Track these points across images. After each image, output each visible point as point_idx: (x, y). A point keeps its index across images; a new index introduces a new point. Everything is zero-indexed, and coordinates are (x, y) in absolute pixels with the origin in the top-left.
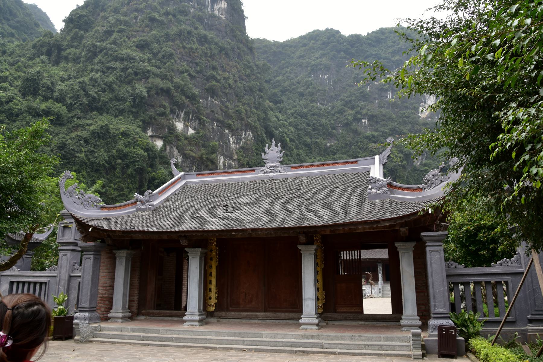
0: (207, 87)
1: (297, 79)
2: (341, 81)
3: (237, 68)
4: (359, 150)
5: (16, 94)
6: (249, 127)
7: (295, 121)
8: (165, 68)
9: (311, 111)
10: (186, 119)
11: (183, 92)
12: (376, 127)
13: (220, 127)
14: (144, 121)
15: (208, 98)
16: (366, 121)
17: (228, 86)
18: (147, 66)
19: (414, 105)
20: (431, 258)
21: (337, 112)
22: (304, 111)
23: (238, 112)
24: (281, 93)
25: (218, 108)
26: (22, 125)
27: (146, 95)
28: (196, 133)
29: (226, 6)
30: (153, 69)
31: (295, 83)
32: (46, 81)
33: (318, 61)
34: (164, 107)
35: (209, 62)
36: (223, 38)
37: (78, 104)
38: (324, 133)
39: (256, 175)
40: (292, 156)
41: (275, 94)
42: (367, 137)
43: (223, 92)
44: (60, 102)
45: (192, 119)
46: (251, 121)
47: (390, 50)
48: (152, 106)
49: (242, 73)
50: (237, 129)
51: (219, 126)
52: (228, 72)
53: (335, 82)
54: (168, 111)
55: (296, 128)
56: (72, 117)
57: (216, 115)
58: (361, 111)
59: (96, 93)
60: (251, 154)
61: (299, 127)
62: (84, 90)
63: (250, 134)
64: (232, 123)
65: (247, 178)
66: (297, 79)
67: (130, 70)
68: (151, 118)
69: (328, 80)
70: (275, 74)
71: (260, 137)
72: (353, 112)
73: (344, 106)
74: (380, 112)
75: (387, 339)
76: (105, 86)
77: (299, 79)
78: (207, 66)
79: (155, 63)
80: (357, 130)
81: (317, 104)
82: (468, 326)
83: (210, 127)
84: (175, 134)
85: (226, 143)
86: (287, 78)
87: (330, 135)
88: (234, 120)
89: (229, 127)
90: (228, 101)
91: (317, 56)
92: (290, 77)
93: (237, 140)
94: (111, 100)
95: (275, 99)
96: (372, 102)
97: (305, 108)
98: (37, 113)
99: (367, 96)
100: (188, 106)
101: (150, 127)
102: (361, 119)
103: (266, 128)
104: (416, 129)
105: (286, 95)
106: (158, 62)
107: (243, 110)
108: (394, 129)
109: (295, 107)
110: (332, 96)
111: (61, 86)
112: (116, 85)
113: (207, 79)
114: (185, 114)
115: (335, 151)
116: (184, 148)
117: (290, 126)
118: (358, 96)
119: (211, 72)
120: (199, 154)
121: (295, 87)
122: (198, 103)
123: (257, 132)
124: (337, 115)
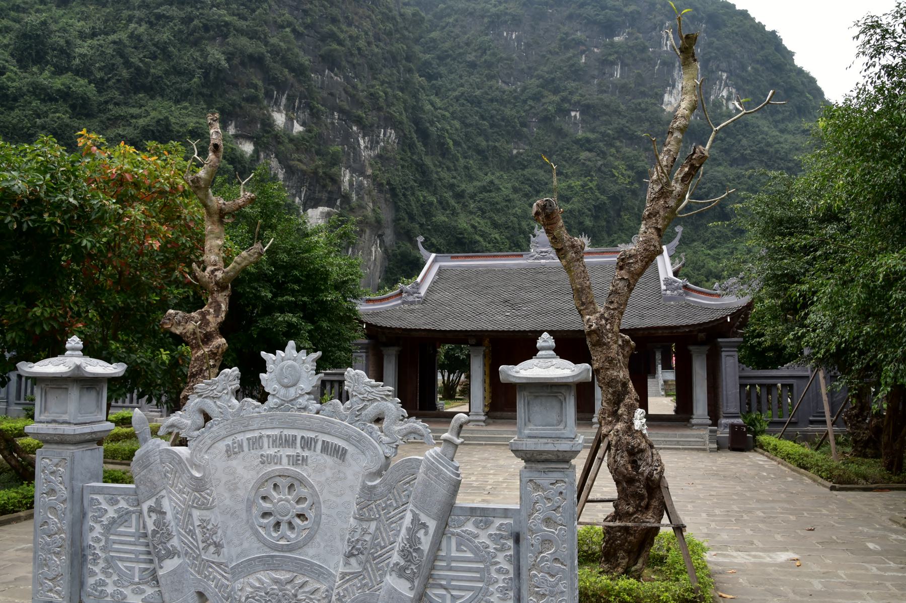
0: (322, 52)
1: (466, 37)
2: (538, 44)
3: (372, 20)
4: (564, 163)
5: (7, 61)
6: (390, 122)
7: (460, 111)
8: (254, 19)
9: (488, 94)
10: (290, 108)
11: (286, 63)
12: (593, 125)
13: (344, 121)
14: (222, 111)
15: (325, 71)
16: (578, 114)
17: (357, 52)
18: (225, 15)
19: (656, 90)
20: (725, 363)
21: (530, 98)
22: (476, 94)
23: (373, 96)
24: (438, 61)
25: (341, 89)
26: (26, 116)
27: (227, 65)
28: (306, 131)
30: (233, 19)
32: (57, 39)
34: (256, 87)
35: (326, 9)
37: (114, 81)
38: (508, 133)
39: (525, 262)
40: (456, 170)
41: (427, 64)
42: (577, 142)
43: (348, 62)
44: (83, 76)
45: (299, 108)
46: (394, 111)
48: (235, 85)
49: (380, 29)
50: (372, 126)
51: (342, 120)
52: (356, 26)
53: (528, 45)
54: (261, 95)
55: (463, 123)
56: (106, 102)
57: (338, 101)
58: (569, 97)
59: (141, 61)
60: (393, 167)
61: (468, 121)
62: (122, 56)
63: (392, 134)
65: (515, 265)
66: (466, 37)
67: (196, 22)
68: (233, 105)
71: (407, 139)
72: (556, 98)
73: (543, 87)
74: (601, 99)
75: (682, 436)
76: (155, 49)
77: (468, 38)
78: (321, 16)
79: (238, 10)
80: (562, 129)
81: (498, 82)
82: (755, 424)
83: (329, 121)
84: (273, 133)
85: (354, 149)
86: (448, 35)
87: (517, 136)
88: (367, 110)
89: (359, 121)
90: (356, 77)
92: (453, 34)
93: (371, 141)
94: (167, 73)
95: (427, 70)
96: (588, 82)
97: (478, 89)
98: (48, 95)
99: (580, 72)
100: (292, 86)
101: (231, 121)
102: (569, 111)
103: (417, 122)
104: (656, 130)
105: (446, 65)
106: (242, 7)
107: (381, 93)
108: (622, 130)
109: (462, 86)
110: (523, 69)
111: (83, 48)
112: (174, 47)
113: (324, 38)
114: (288, 99)
115: (526, 163)
116: (289, 156)
117: (454, 118)
118: (566, 72)
119: (328, 27)
120: (313, 166)
122: (309, 80)
123: (403, 131)
124: (530, 102)
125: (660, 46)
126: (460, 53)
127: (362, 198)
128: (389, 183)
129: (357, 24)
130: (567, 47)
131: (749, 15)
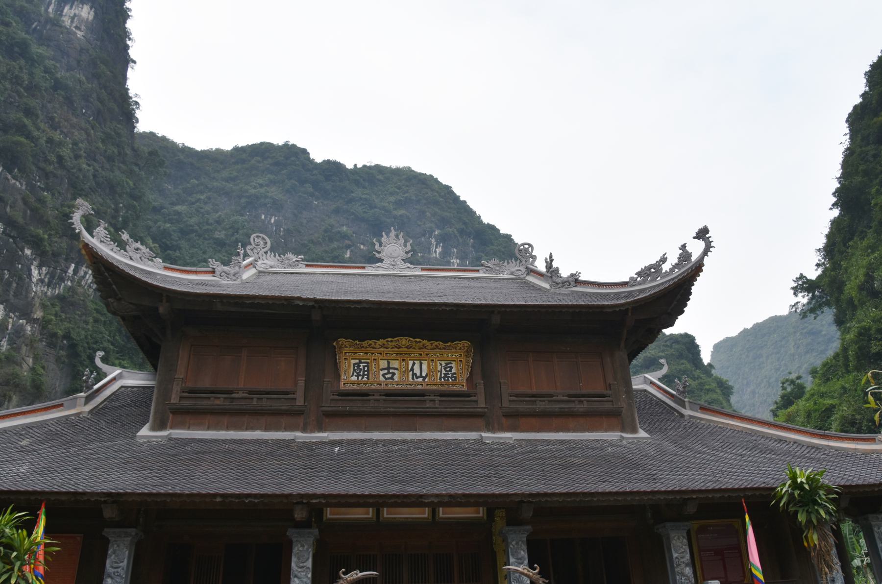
1: (217, 215)
2: (300, 232)
3: (88, 135)
13: (12, 237)
24: (179, 234)
25: (19, 197)
29: (91, 17)
31: (211, 221)
33: (262, 190)
43: (39, 168)
47: (392, 199)
49: (97, 148)
50: (55, 255)
52: (62, 132)
53: (288, 231)
57: (8, 209)
60: (80, 316)
64: (46, 237)
69: (276, 226)
70: (174, 200)
77: (220, 216)
78: (11, 103)
85: (20, 278)
86: (197, 210)
89: (36, 244)
90: (47, 189)
91: (260, 181)
93: (52, 276)
95: (164, 240)
121: (210, 227)
125: (430, 252)
126: (208, 229)
127: (18, 349)
128: (67, 336)
129: (65, 130)
130: (331, 240)
131: (512, 240)
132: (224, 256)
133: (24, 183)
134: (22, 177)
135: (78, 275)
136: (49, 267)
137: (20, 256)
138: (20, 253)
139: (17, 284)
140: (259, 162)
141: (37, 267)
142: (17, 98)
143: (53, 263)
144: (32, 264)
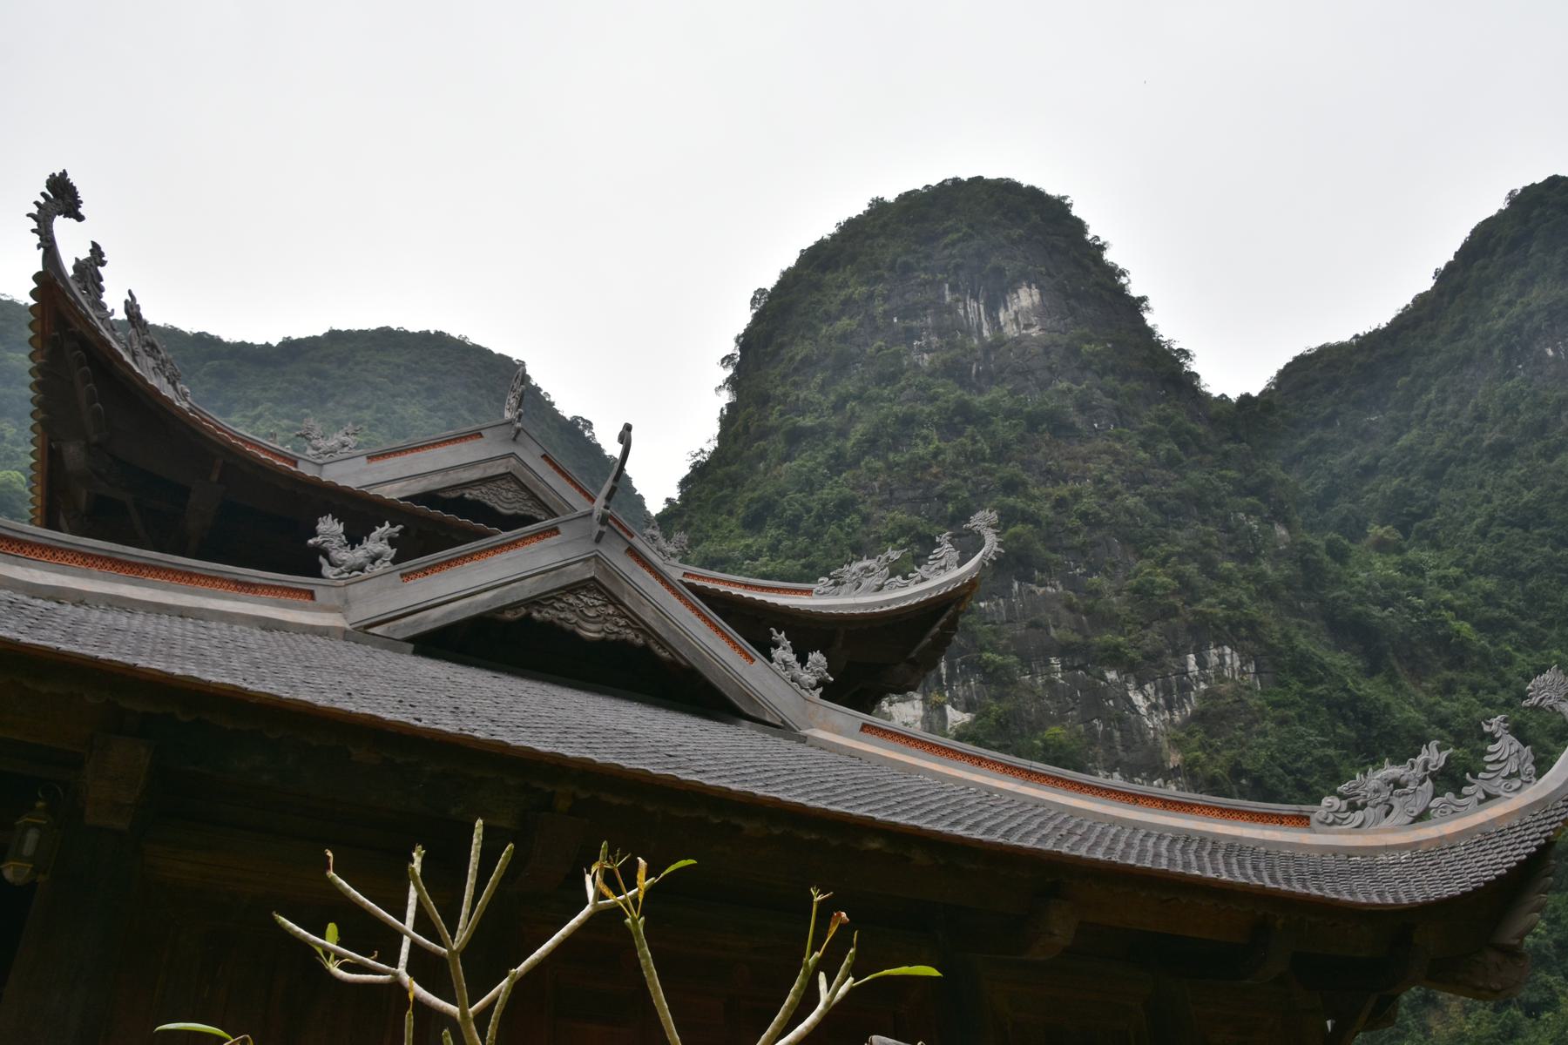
3: (1115, 454)
6: (1203, 633)
7: (1497, 553)
17: (1078, 523)
23: (1142, 593)
24: (1429, 483)
25: (1058, 606)
29: (1036, 298)
33: (1517, 309)
35: (991, 475)
36: (1043, 386)
45: (951, 678)
61: (1522, 567)
77: (1476, 406)
83: (1040, 680)
85: (1121, 720)
86: (1437, 424)
89: (1114, 657)
90: (1093, 569)
91: (1505, 297)
93: (1167, 692)
132: (1520, 469)
133: (1058, 582)
134: (1051, 577)
135: (1210, 666)
136: (1154, 680)
137: (1104, 688)
138: (1102, 683)
139: (1121, 730)
140: (1485, 267)
141: (1136, 689)
142: (989, 479)
143: (1157, 671)
144: (1127, 690)
